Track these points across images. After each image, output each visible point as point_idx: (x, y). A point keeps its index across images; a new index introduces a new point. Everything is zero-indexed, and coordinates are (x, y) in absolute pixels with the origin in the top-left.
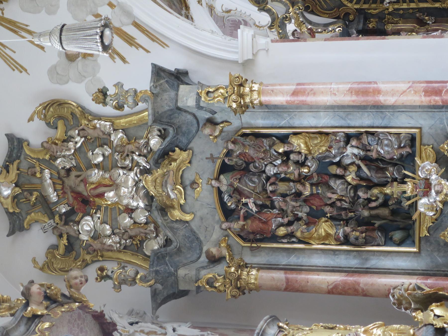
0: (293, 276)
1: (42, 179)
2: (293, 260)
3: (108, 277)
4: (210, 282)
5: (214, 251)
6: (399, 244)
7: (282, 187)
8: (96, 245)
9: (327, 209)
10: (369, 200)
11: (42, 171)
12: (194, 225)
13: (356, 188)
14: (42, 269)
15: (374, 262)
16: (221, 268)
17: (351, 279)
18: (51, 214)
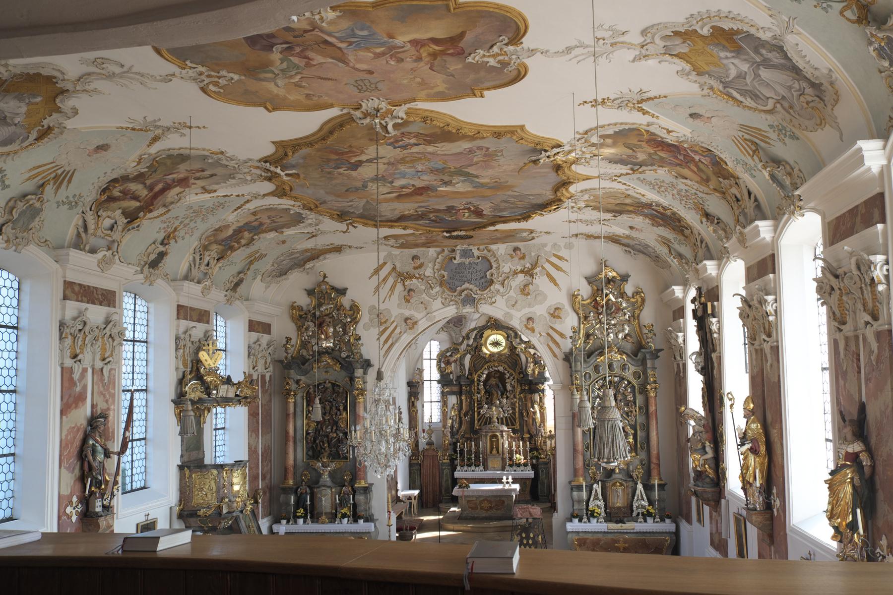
0: (291, 416)
1: (329, 304)
2: (299, 413)
3: (287, 342)
4: (288, 383)
5: (301, 382)
6: (307, 454)
7: (328, 408)
8: (303, 330)
9: (319, 426)
10: (323, 442)
11: (333, 304)
12: (311, 372)
13: (328, 436)
14: (292, 306)
15: (299, 445)
16: (294, 386)
17: (291, 439)
18: (314, 308)
